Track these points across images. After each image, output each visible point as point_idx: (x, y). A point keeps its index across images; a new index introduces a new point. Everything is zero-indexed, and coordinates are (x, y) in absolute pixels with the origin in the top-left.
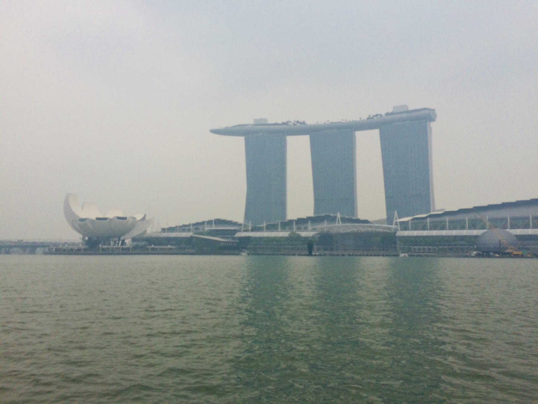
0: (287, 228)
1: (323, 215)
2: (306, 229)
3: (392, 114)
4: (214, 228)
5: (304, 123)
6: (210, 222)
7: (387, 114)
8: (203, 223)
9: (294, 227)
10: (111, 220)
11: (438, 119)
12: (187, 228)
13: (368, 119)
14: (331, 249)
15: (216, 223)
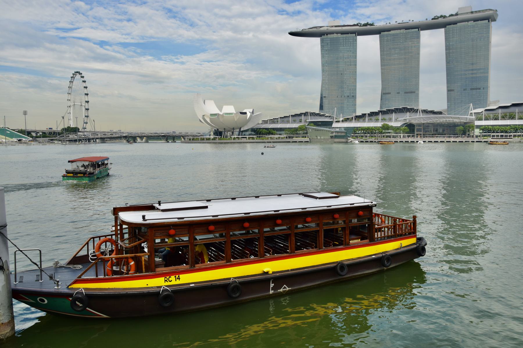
0: (374, 118)
1: (401, 107)
2: (390, 120)
3: (457, 14)
4: (310, 119)
5: (372, 25)
6: (306, 114)
7: (452, 15)
8: (300, 115)
9: (380, 117)
10: (222, 115)
11: (497, 20)
12: (276, 120)
13: (432, 19)
14: (413, 136)
15: (310, 115)
